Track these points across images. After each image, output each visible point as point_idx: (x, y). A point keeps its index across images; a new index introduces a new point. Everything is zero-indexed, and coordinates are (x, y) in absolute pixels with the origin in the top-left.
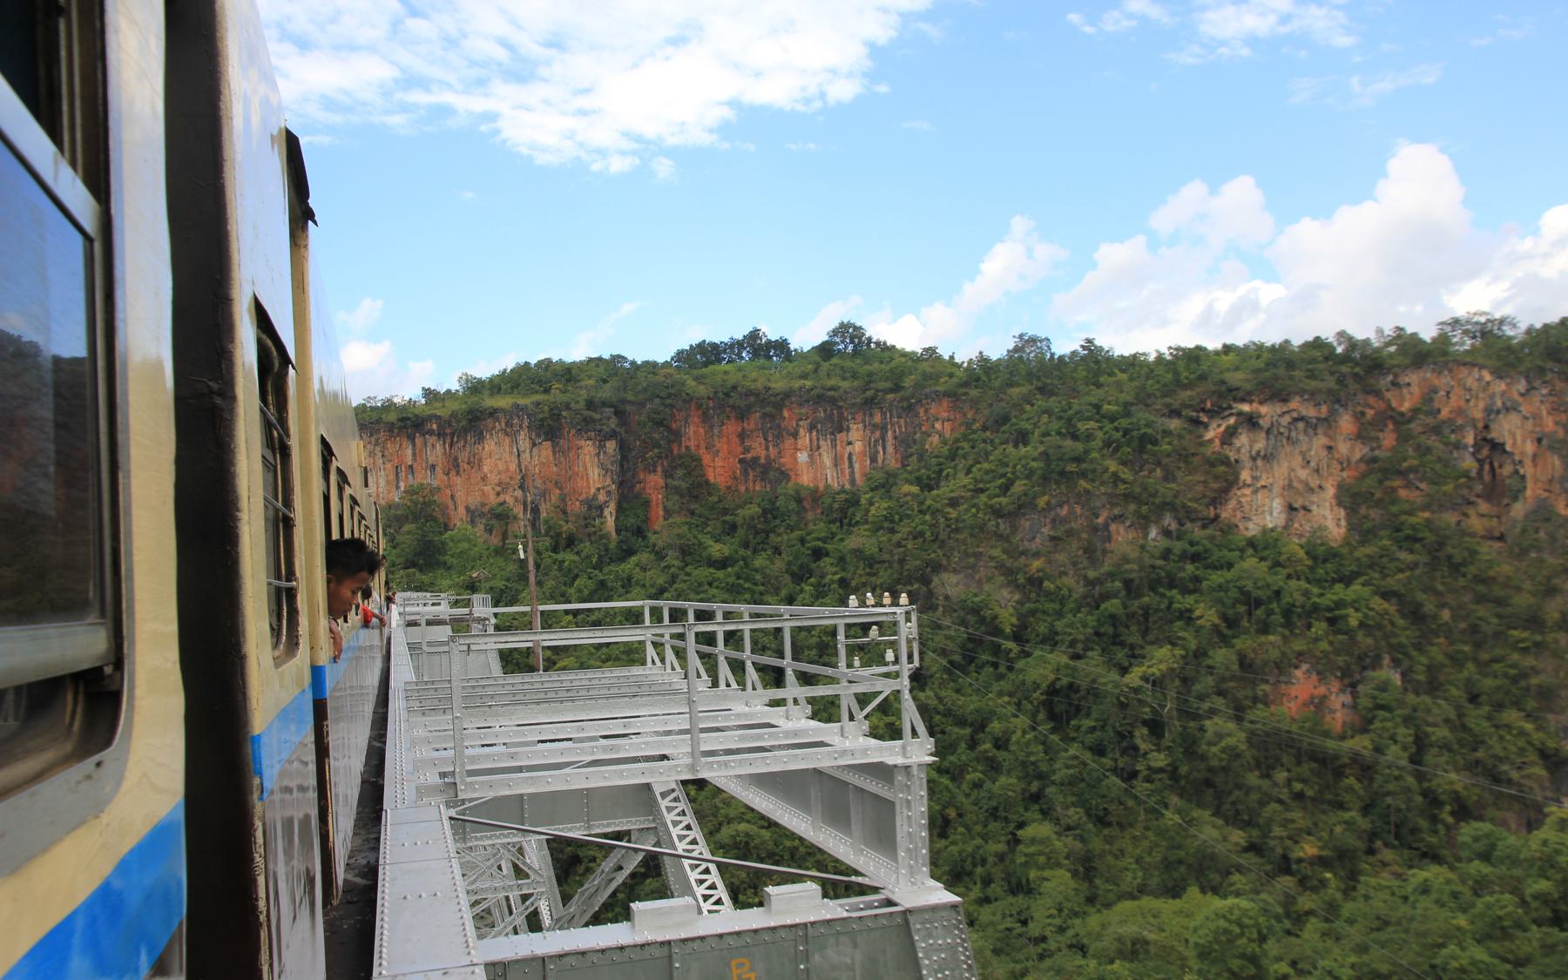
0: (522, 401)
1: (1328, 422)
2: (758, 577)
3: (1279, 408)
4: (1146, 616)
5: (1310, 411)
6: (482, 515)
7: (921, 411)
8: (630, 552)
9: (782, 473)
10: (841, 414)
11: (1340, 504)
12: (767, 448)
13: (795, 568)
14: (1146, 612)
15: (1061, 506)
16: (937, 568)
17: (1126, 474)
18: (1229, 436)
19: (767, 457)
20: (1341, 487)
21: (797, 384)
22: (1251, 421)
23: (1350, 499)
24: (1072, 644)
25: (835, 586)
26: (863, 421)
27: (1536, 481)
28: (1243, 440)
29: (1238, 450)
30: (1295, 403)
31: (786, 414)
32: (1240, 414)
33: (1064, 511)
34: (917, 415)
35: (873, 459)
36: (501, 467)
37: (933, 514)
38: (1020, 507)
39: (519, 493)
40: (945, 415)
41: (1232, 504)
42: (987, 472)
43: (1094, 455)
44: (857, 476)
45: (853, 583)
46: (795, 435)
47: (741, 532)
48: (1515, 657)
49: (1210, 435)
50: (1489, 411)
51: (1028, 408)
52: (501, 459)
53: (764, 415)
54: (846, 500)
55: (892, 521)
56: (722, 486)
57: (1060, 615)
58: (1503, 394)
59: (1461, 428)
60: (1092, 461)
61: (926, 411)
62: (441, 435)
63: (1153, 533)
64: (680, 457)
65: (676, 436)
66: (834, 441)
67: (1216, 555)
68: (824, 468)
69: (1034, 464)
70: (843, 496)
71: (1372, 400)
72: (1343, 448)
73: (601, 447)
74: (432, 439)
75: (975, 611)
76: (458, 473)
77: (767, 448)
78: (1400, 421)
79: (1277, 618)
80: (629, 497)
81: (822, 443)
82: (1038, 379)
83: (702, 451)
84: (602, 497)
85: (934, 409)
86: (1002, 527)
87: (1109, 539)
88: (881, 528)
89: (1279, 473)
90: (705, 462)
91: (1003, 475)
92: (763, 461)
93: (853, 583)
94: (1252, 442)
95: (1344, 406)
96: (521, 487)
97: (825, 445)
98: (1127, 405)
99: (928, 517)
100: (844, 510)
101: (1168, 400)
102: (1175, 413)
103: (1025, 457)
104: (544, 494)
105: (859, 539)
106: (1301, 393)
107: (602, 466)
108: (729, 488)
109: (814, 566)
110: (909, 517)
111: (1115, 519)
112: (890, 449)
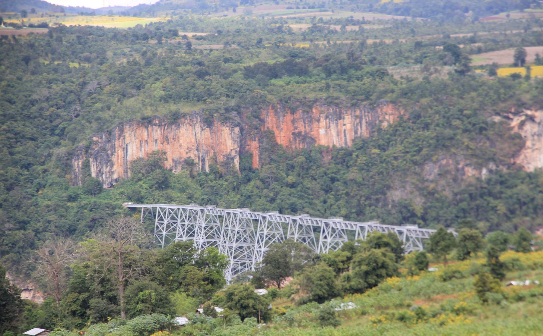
2: (310, 192)
4: (477, 209)
6: (180, 163)
7: (379, 110)
9: (313, 139)
12: (305, 127)
13: (325, 187)
14: (478, 207)
16: (389, 187)
17: (472, 145)
18: (522, 125)
19: (305, 131)
22: (532, 119)
24: (446, 220)
25: (343, 196)
26: (351, 114)
29: (526, 132)
31: (314, 110)
32: (527, 115)
34: (377, 112)
35: (356, 133)
36: (188, 140)
37: (387, 163)
38: (425, 160)
39: (196, 152)
40: (390, 112)
41: (522, 157)
42: (410, 143)
43: (458, 137)
44: (348, 141)
45: (352, 194)
46: (319, 121)
47: (297, 169)
51: (430, 110)
54: (345, 154)
55: (368, 166)
56: (284, 145)
57: (442, 208)
60: (458, 140)
61: (382, 110)
63: (484, 171)
64: (265, 132)
65: (262, 121)
66: (337, 124)
69: (431, 141)
70: (343, 152)
73: (233, 130)
75: (405, 207)
76: (168, 143)
77: (305, 127)
79: (531, 210)
80: (244, 153)
81: (331, 125)
82: (435, 94)
84: (233, 154)
85: (385, 109)
87: (464, 174)
88: (363, 169)
90: (276, 134)
92: (303, 134)
93: (352, 194)
96: (197, 150)
97: (333, 126)
98: (476, 110)
99: (384, 165)
100: (343, 157)
101: (495, 108)
103: (428, 137)
104: (207, 152)
105: (353, 174)
108: (287, 146)
109: (332, 186)
110: (376, 164)
111: (467, 165)
112: (364, 128)
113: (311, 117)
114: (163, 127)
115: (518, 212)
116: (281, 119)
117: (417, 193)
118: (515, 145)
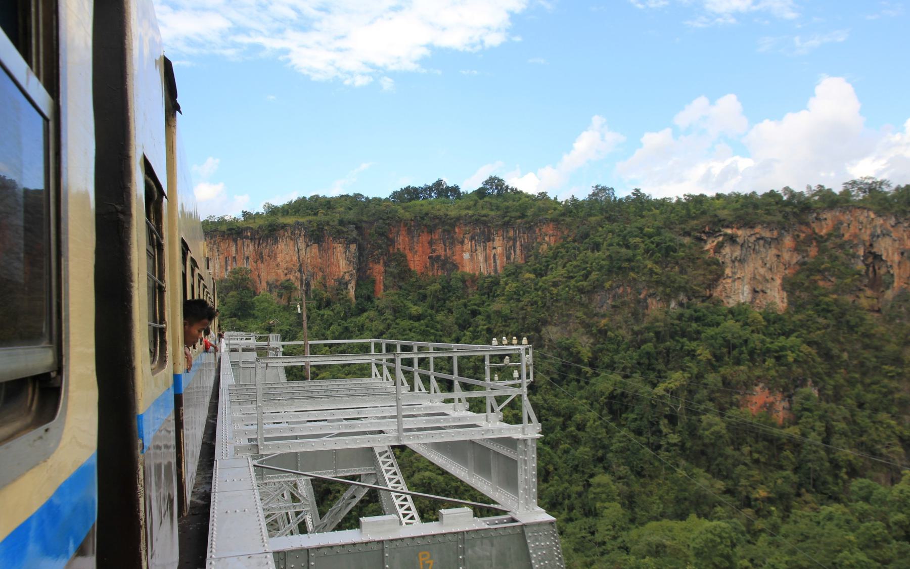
0: (301, 220)
1: (777, 240)
2: (439, 326)
3: (749, 232)
5: (767, 234)
6: (276, 287)
7: (537, 230)
8: (363, 310)
10: (489, 231)
11: (784, 289)
12: (445, 250)
13: (461, 322)
14: (668, 350)
15: (618, 287)
16: (545, 323)
17: (657, 269)
18: (719, 248)
19: (446, 255)
20: (784, 279)
21: (464, 212)
22: (732, 239)
23: (790, 286)
24: (624, 369)
25: (484, 332)
26: (503, 235)
27: (900, 278)
28: (727, 250)
29: (724, 256)
30: (758, 229)
31: (457, 230)
32: (725, 235)
33: (620, 291)
34: (534, 233)
35: (508, 258)
36: (288, 259)
37: (543, 291)
38: (594, 287)
39: (298, 274)
41: (720, 288)
42: (575, 267)
43: (639, 257)
44: (498, 268)
45: (495, 331)
46: (462, 243)
47: (429, 299)
48: (886, 381)
49: (707, 247)
50: (873, 236)
51: (600, 229)
52: (288, 254)
53: (444, 231)
55: (519, 295)
57: (617, 352)
58: (881, 226)
59: (856, 245)
60: (638, 261)
61: (540, 230)
62: (252, 239)
63: (673, 304)
64: (394, 254)
65: (392, 242)
67: (710, 318)
68: (479, 262)
69: (603, 263)
70: (490, 279)
71: (803, 228)
72: (786, 256)
73: (347, 247)
74: (247, 242)
75: (567, 349)
76: (262, 262)
77: (445, 250)
78: (820, 240)
79: (746, 356)
80: (363, 278)
81: (478, 248)
82: (607, 212)
83: (407, 251)
84: (347, 277)
85: (544, 228)
86: (584, 299)
87: (647, 307)
88: (512, 298)
89: (748, 270)
90: (408, 258)
91: (585, 269)
92: (443, 258)
93: (495, 331)
94: (732, 252)
95: (788, 231)
96: (300, 271)
97: (480, 249)
98: (658, 228)
99: (540, 293)
100: (490, 288)
101: (683, 226)
102: (687, 234)
103: (598, 258)
104: (313, 275)
105: (498, 305)
106: (762, 223)
107: (347, 259)
108: (422, 273)
109: (472, 320)
110: (528, 292)
111: (651, 295)
112: (518, 252)
113: (453, 237)
114: (257, 242)
115: (726, 359)
116: (415, 239)
117: (582, 330)
118: (711, 272)
